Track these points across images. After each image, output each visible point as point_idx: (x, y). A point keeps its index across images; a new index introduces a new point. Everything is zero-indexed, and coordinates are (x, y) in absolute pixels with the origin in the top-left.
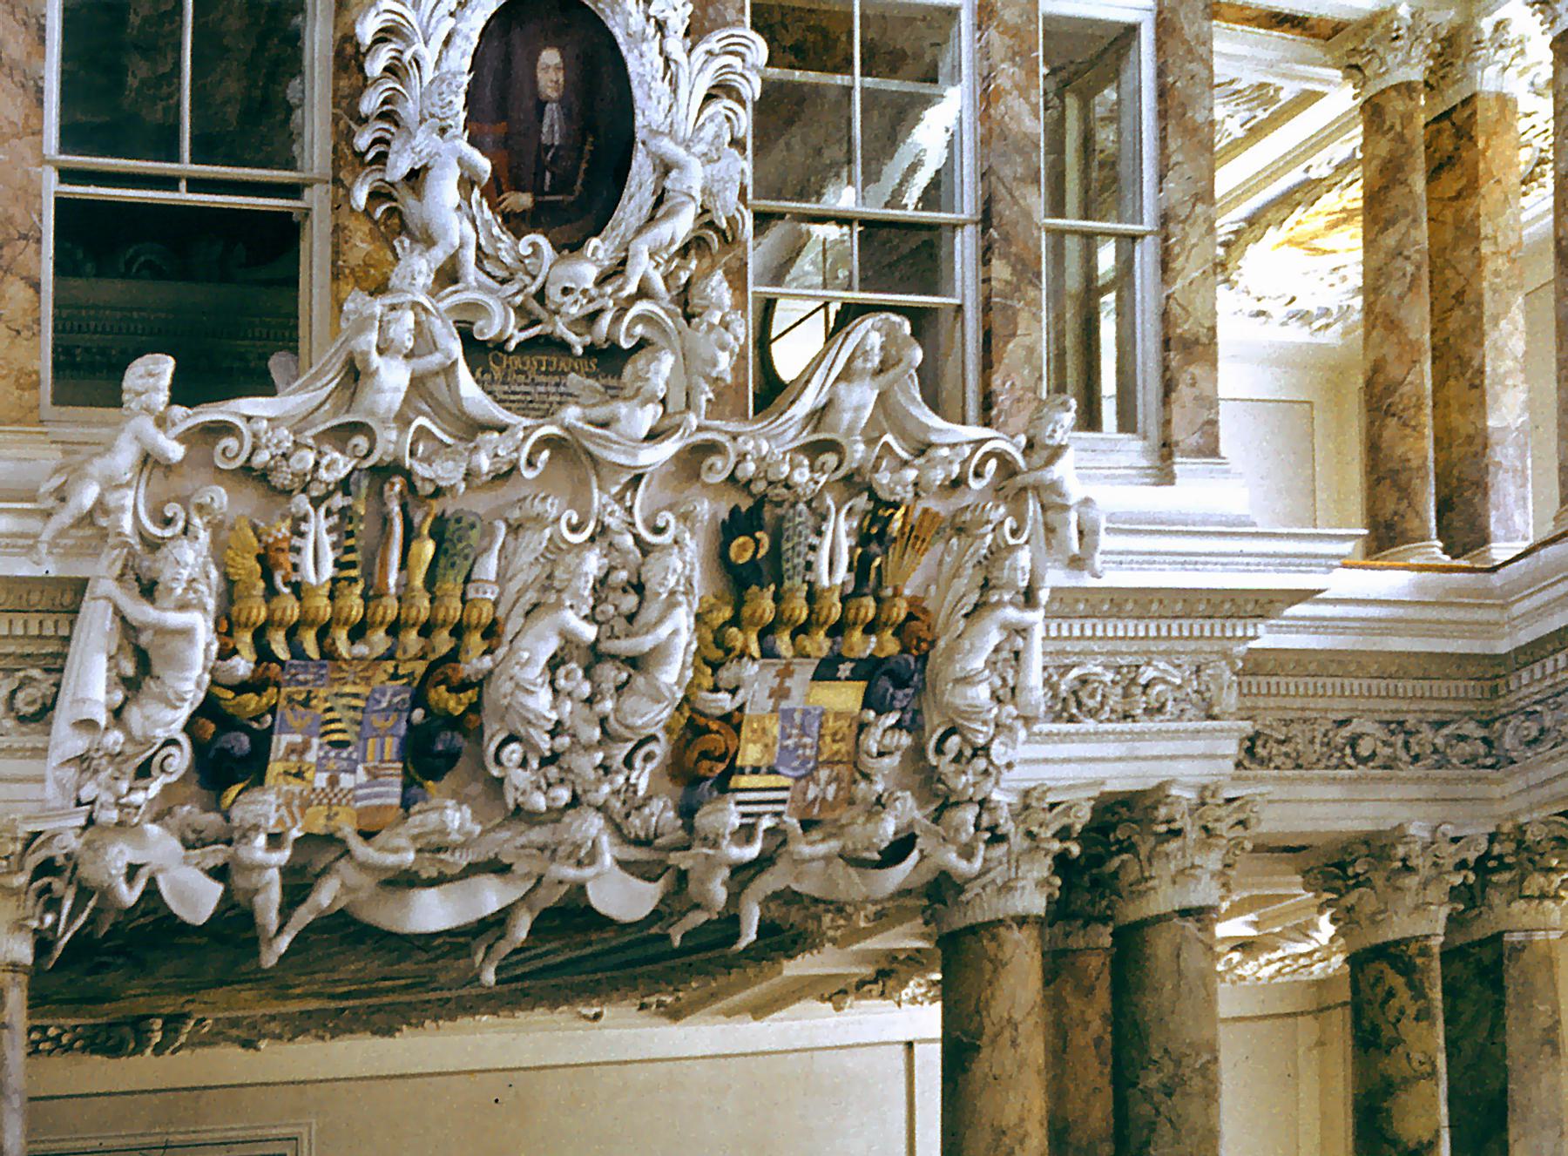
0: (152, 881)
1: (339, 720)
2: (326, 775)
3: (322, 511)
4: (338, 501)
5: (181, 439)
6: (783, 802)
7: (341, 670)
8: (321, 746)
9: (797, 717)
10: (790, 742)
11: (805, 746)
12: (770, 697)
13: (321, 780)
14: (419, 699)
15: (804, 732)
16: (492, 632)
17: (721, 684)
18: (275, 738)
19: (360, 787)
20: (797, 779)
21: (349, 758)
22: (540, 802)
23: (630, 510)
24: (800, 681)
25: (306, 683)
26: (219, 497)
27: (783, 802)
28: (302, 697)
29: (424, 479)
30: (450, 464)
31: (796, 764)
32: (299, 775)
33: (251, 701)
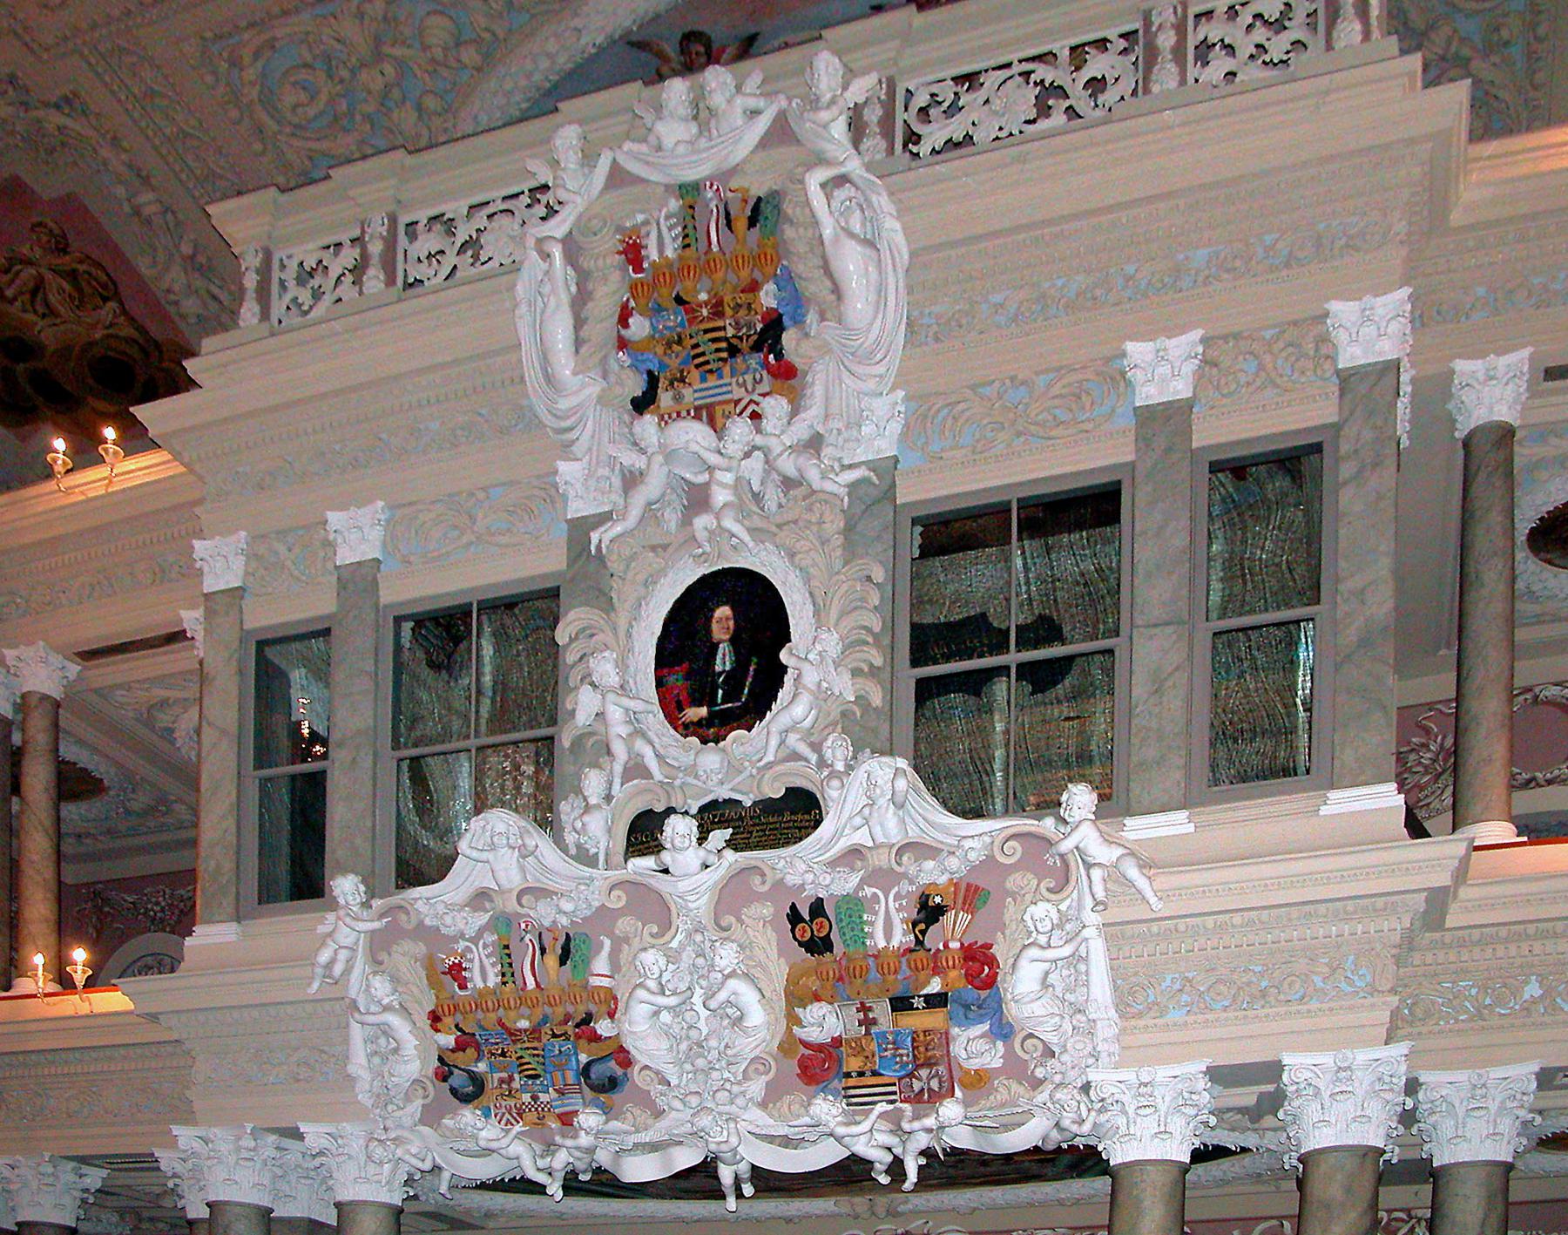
13: (526, 1098)
20: (900, 1079)
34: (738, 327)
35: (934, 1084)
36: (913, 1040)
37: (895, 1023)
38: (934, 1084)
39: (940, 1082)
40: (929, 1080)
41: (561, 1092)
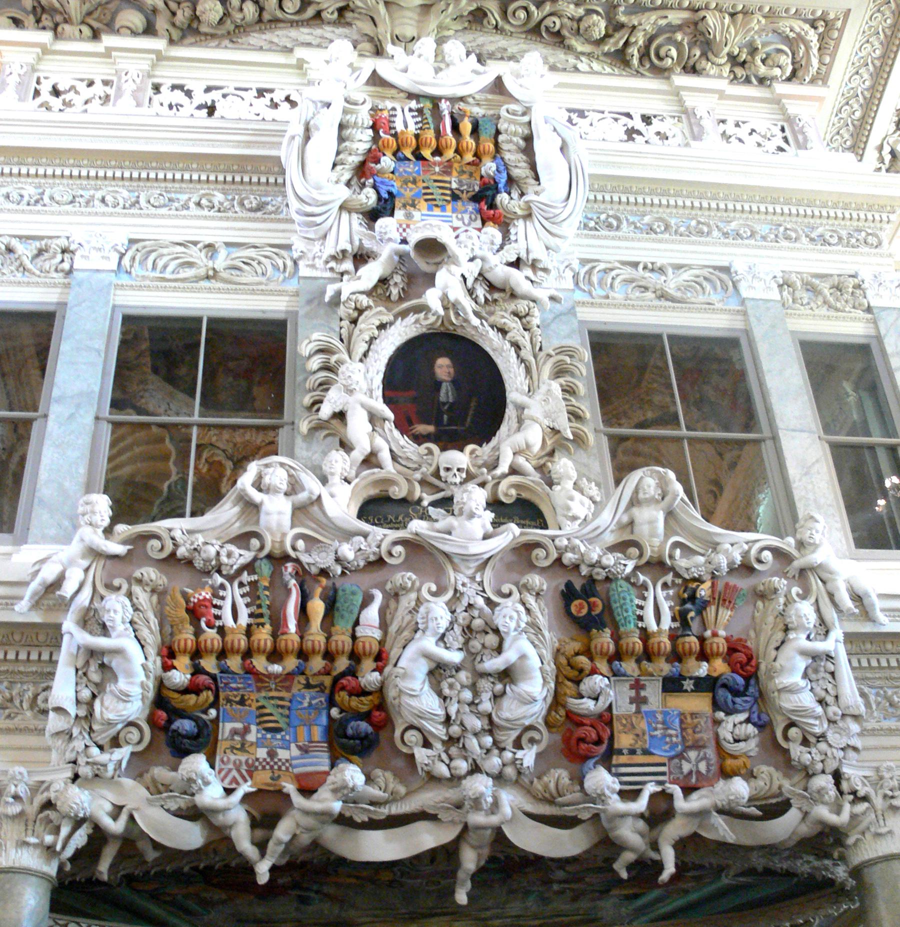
0: (131, 818)
1: (271, 715)
2: (265, 750)
3: (236, 584)
4: (245, 577)
5: (124, 542)
6: (663, 774)
7: (262, 681)
8: (258, 731)
9: (660, 717)
10: (658, 733)
11: (671, 736)
12: (631, 703)
13: (262, 753)
14: (331, 703)
15: (666, 726)
16: (380, 658)
17: (584, 693)
18: (221, 725)
19: (293, 758)
20: (671, 758)
21: (283, 739)
22: (443, 770)
23: (481, 583)
24: (653, 692)
25: (237, 689)
26: (151, 573)
27: (663, 774)
28: (238, 699)
29: (308, 564)
30: (324, 554)
31: (667, 747)
32: (242, 749)
33: (192, 699)
34: (460, 183)
35: (703, 767)
36: (681, 722)
37: (664, 703)
38: (703, 767)
39: (708, 765)
40: (698, 761)
41: (304, 750)
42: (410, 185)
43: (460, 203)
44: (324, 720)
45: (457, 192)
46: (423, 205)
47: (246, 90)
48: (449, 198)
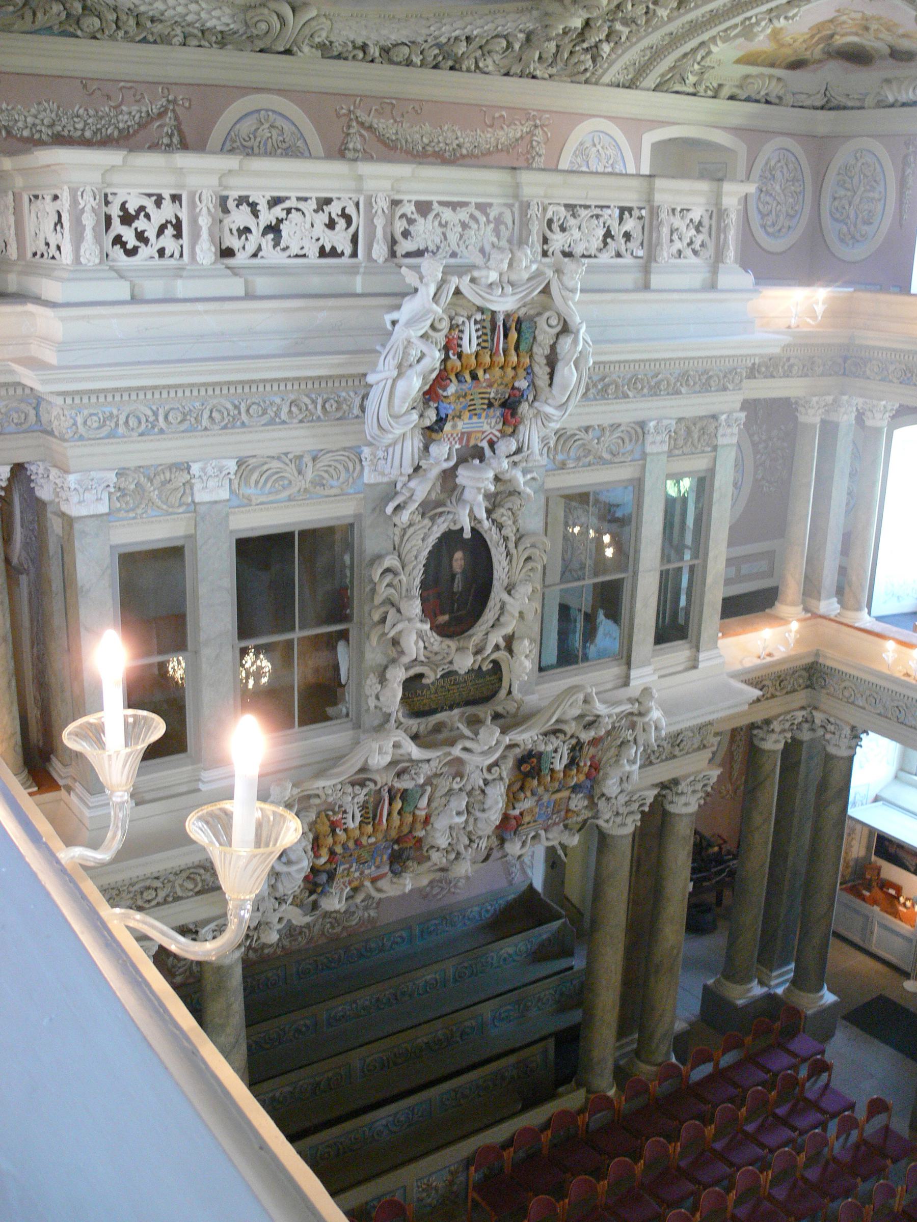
13: (357, 874)
16: (427, 821)
41: (378, 867)
42: (461, 399)
43: (492, 410)
44: (390, 851)
45: (492, 401)
46: (467, 414)
47: (305, 199)
48: (485, 407)
